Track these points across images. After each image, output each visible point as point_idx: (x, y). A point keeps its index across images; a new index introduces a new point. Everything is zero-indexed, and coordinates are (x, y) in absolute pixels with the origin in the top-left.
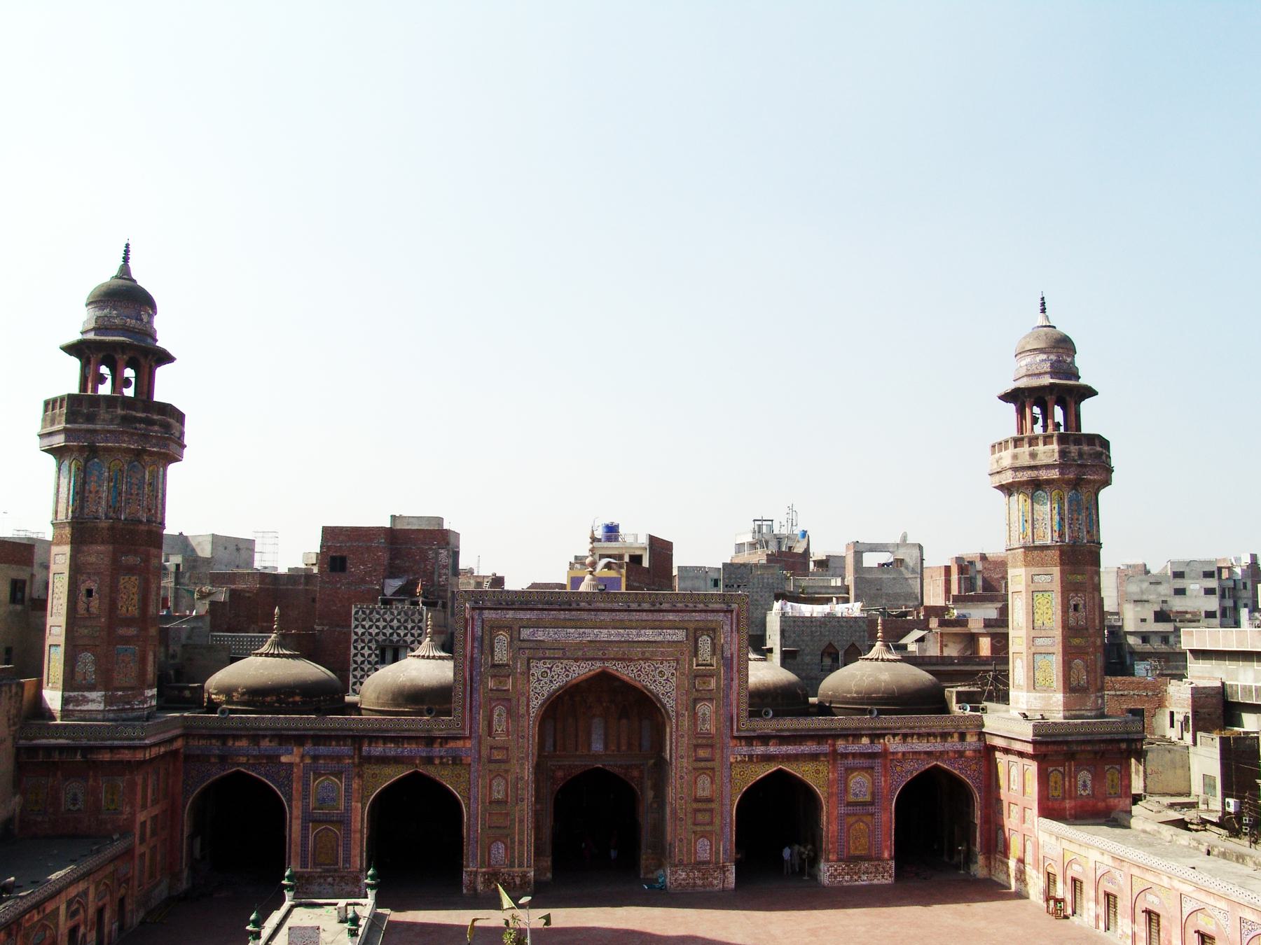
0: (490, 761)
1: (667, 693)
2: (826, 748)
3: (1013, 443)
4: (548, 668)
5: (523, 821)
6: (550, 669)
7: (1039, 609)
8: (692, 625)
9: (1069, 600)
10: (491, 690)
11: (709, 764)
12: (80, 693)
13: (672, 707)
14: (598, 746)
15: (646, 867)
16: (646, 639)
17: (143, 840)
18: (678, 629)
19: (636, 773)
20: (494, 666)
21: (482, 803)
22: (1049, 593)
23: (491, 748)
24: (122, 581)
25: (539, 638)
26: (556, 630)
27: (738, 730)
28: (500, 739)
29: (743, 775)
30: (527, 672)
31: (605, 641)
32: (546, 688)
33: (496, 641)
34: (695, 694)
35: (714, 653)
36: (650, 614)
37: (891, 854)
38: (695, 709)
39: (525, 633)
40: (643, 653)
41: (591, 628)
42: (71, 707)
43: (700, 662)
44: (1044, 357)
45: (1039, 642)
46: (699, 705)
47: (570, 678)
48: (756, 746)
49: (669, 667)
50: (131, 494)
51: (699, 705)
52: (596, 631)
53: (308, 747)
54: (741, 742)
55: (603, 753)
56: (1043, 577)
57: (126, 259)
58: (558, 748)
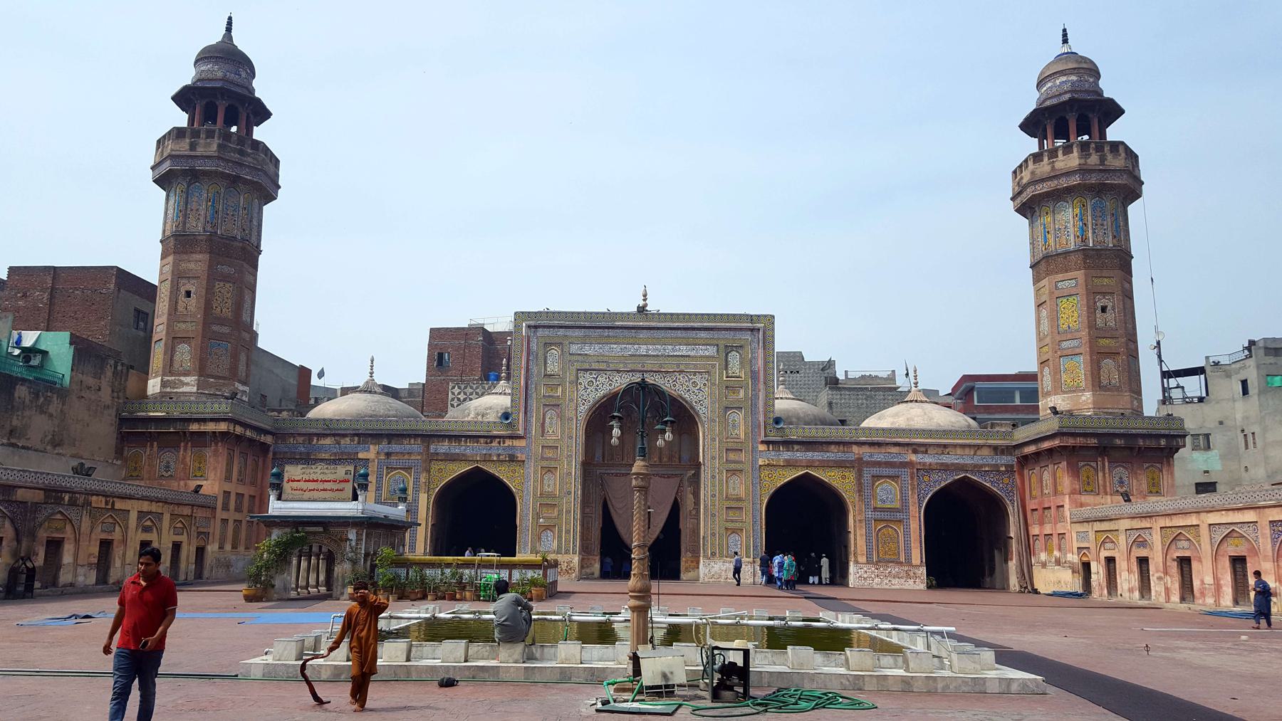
0: (543, 459)
1: (700, 401)
3: (1032, 160)
4: (594, 378)
5: (570, 512)
7: (1064, 313)
8: (722, 343)
9: (1095, 303)
11: (739, 466)
12: (177, 378)
15: (686, 568)
17: (226, 507)
18: (707, 345)
22: (1074, 297)
24: (217, 287)
28: (550, 438)
30: (576, 382)
32: (592, 395)
37: (922, 561)
39: (574, 348)
40: (678, 365)
42: (168, 390)
44: (1064, 79)
45: (1065, 344)
46: (729, 413)
50: (228, 214)
51: (729, 413)
52: (636, 346)
53: (384, 446)
54: (768, 448)
56: (1067, 283)
57: (229, 29)
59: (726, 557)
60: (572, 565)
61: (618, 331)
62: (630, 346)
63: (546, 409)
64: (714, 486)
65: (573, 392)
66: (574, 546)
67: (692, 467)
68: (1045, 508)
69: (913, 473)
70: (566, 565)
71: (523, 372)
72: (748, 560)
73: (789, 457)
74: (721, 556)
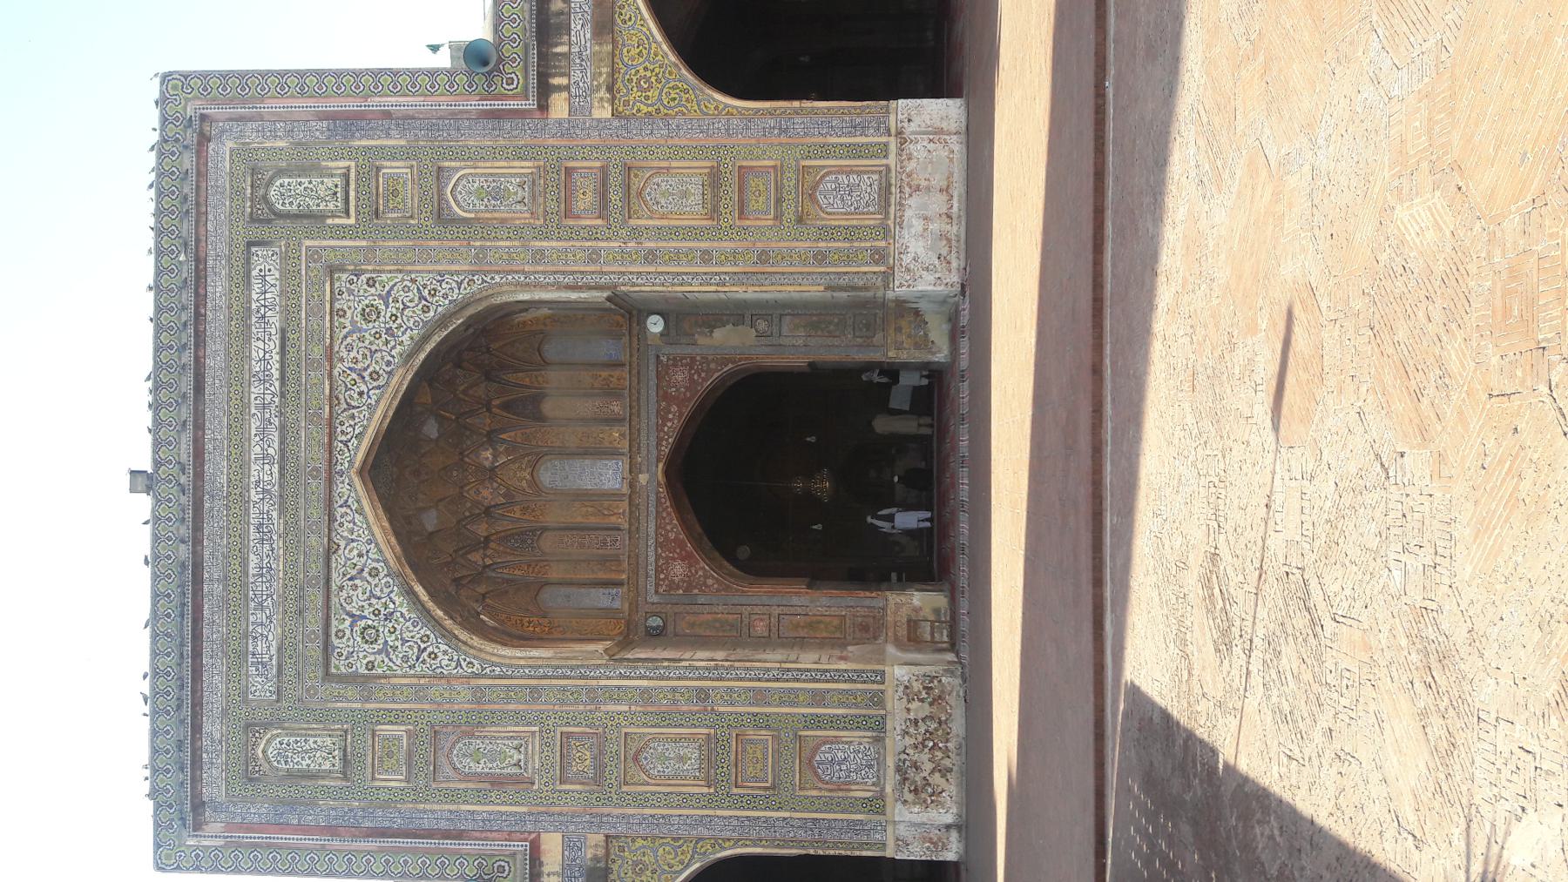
0: (598, 779)
1: (422, 298)
4: (352, 626)
11: (615, 179)
13: (459, 284)
14: (608, 476)
16: (277, 357)
19: (680, 376)
20: (344, 773)
21: (710, 802)
25: (273, 651)
26: (252, 604)
29: (648, 80)
30: (363, 681)
31: (281, 469)
36: (211, 347)
38: (465, 220)
41: (247, 510)
47: (379, 565)
49: (351, 292)
52: (254, 496)
54: (560, 88)
55: (627, 460)
58: (613, 576)
59: (887, 217)
60: (917, 686)
61: (206, 553)
63: (448, 770)
64: (676, 256)
65: (394, 687)
66: (859, 676)
67: (635, 332)
70: (915, 705)
72: (893, 147)
73: (588, 28)
74: (886, 232)
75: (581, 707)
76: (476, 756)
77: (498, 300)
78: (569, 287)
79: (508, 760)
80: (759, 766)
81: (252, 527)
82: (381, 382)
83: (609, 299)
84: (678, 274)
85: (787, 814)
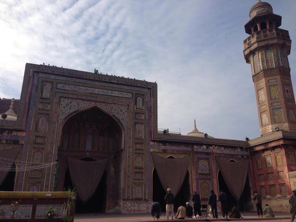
0: (35, 143)
2: (189, 149)
4: (69, 102)
5: (49, 174)
6: (71, 103)
8: (134, 92)
9: (285, 88)
10: (39, 109)
14: (89, 147)
16: (115, 95)
23: (36, 137)
26: (74, 86)
27: (153, 138)
30: (59, 103)
31: (97, 94)
33: (44, 88)
34: (136, 121)
35: (143, 104)
38: (135, 127)
39: (59, 86)
43: (138, 108)
44: (263, 9)
45: (274, 104)
48: (161, 146)
49: (125, 108)
52: (93, 89)
54: (155, 143)
56: (273, 80)
61: (84, 80)
62: (90, 89)
68: (268, 173)
69: (213, 158)
71: (28, 95)
75: (50, 141)
76: (43, 121)
77: (123, 131)
78: (124, 142)
79: (41, 127)
80: (34, 175)
81: (87, 88)
82: (110, 111)
83: (122, 149)
84: (126, 161)
85: (24, 180)
